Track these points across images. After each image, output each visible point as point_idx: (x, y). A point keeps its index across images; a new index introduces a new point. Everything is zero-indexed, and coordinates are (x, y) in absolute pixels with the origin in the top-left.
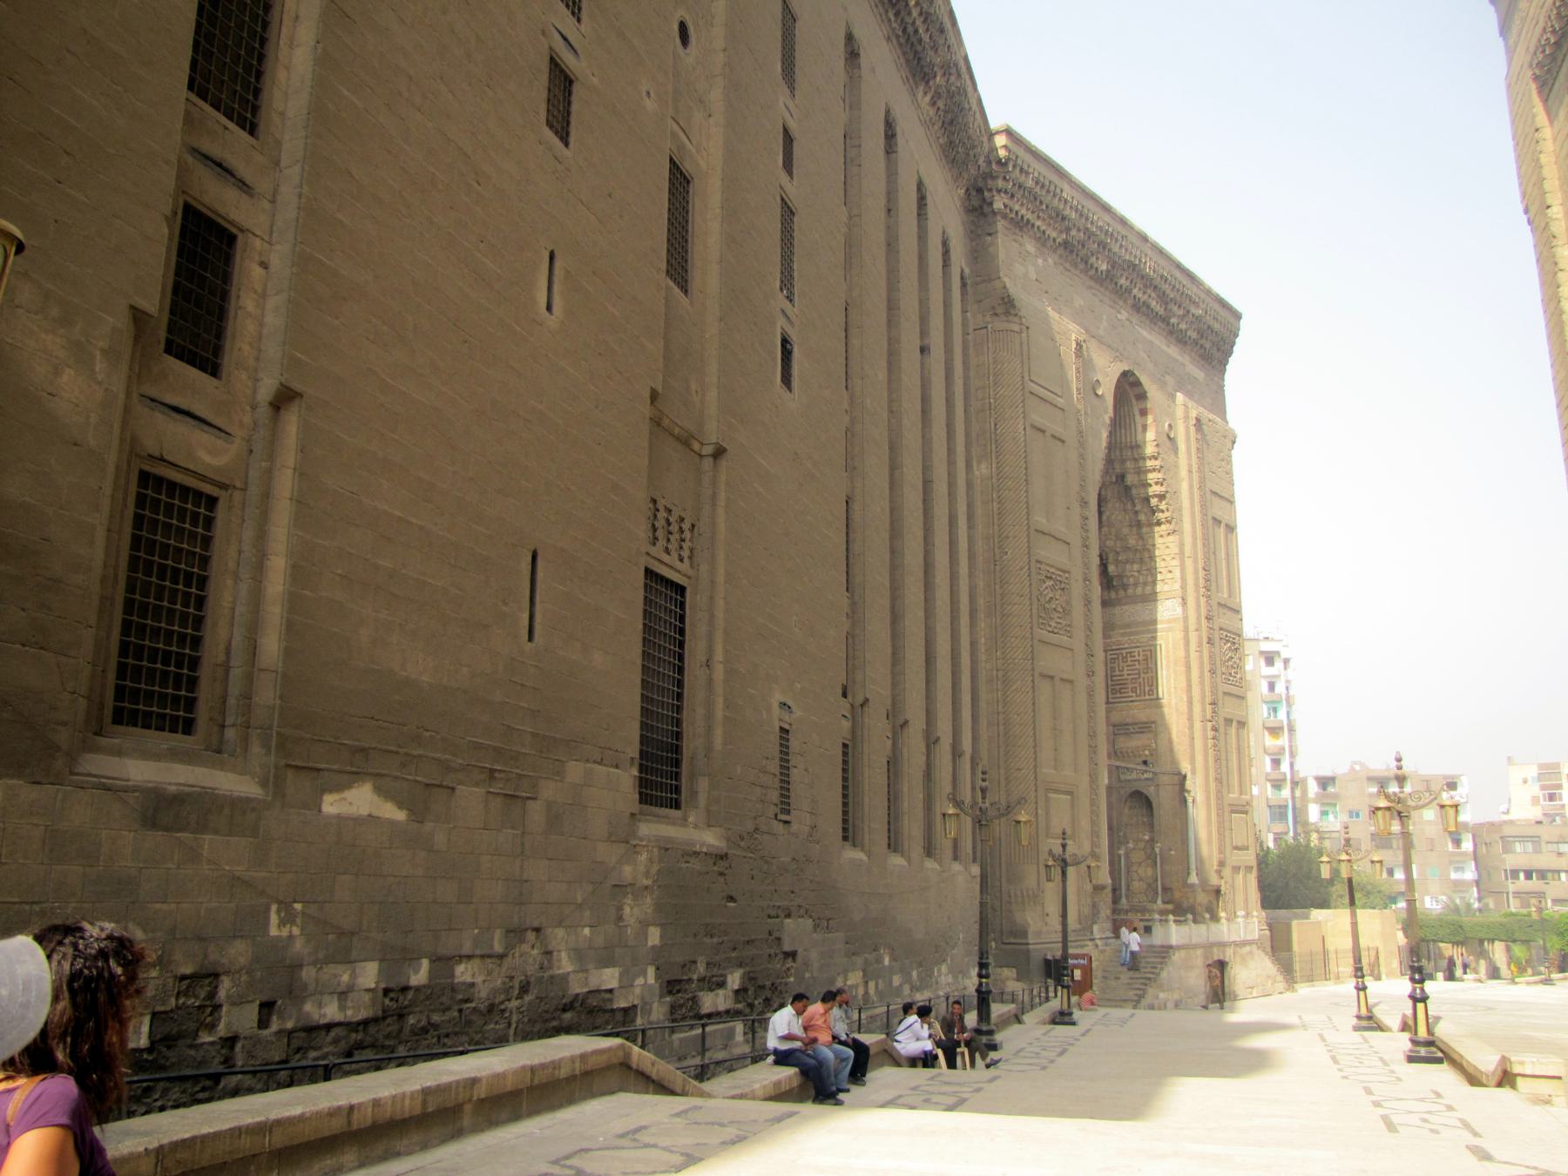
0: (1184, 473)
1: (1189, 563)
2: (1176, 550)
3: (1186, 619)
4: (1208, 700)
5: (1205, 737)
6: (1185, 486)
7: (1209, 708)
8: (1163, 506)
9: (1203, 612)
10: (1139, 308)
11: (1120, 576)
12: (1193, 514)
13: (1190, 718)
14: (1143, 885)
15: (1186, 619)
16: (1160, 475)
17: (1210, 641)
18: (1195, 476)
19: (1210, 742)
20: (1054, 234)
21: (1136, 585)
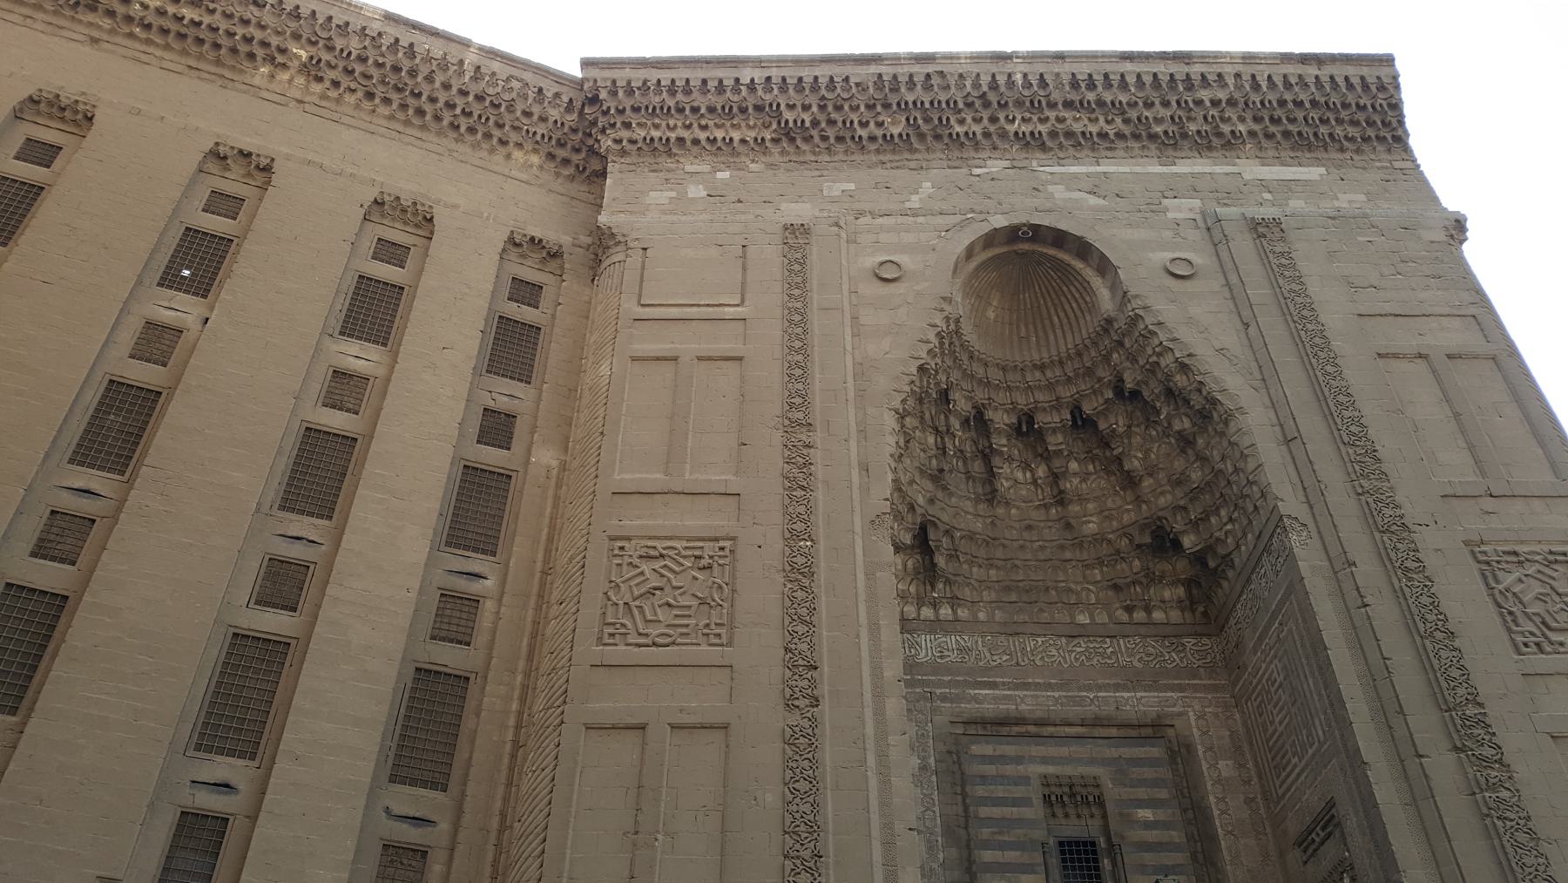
10: (1032, 143)
11: (1210, 548)
20: (753, 134)
21: (1238, 546)
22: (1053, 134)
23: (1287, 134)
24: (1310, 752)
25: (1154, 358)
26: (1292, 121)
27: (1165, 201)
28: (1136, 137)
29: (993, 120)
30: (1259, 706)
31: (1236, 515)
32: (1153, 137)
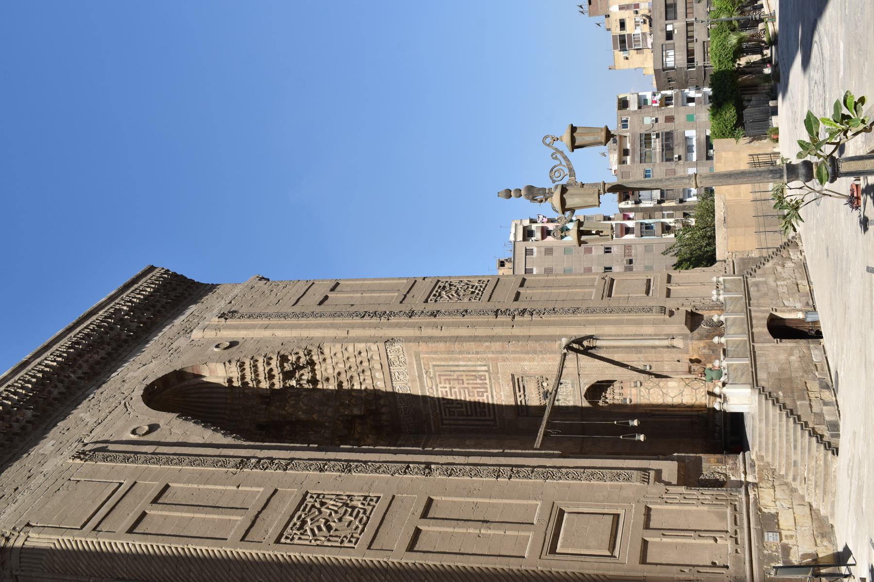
0: (267, 333)
1: (354, 333)
2: (338, 346)
3: (408, 340)
4: (491, 318)
5: (530, 324)
6: (279, 333)
7: (501, 318)
8: (292, 358)
9: (404, 320)
12: (307, 327)
13: (508, 339)
14: (687, 391)
15: (408, 340)
16: (261, 360)
17: (434, 314)
18: (274, 321)
19: (536, 318)
22: (91, 368)
23: (163, 307)
24: (487, 381)
25: (267, 369)
26: (158, 301)
27: (172, 346)
28: (120, 346)
29: (62, 382)
30: (450, 412)
31: (362, 378)
32: (126, 341)
